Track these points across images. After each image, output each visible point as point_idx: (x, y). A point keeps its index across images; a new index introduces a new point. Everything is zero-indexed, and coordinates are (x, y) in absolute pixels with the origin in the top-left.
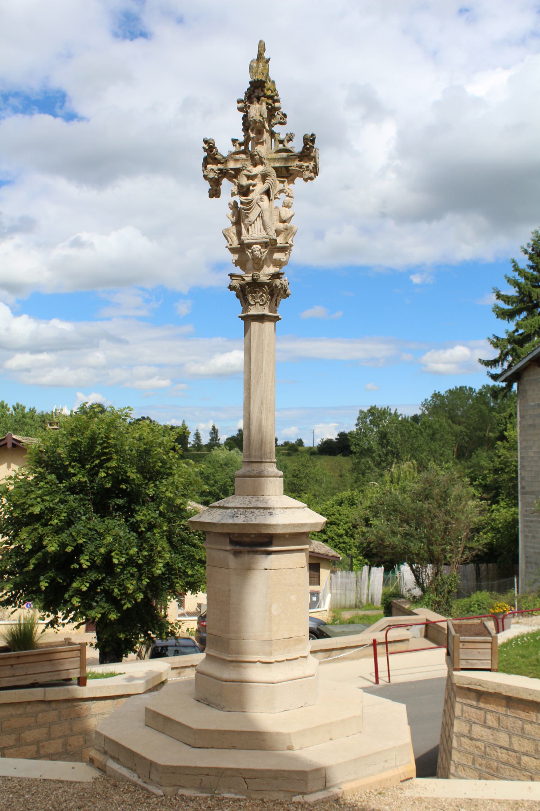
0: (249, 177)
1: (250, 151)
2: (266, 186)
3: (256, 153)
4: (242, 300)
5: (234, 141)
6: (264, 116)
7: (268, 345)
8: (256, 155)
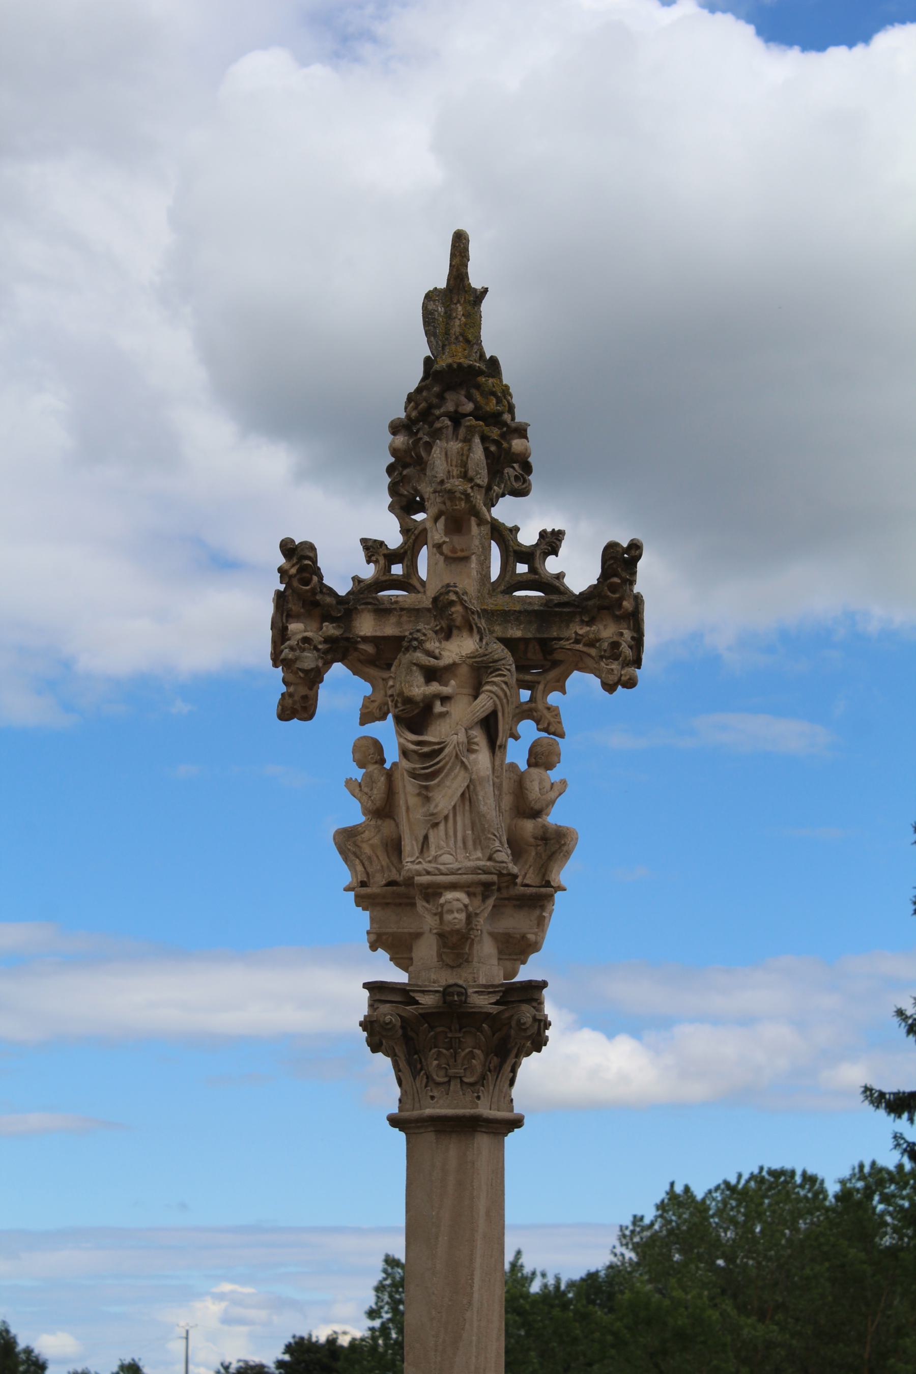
0: (432, 674)
1: (423, 583)
2: (484, 703)
3: (453, 597)
4: (403, 1064)
5: (372, 549)
6: (479, 481)
7: (488, 1213)
8: (452, 603)
